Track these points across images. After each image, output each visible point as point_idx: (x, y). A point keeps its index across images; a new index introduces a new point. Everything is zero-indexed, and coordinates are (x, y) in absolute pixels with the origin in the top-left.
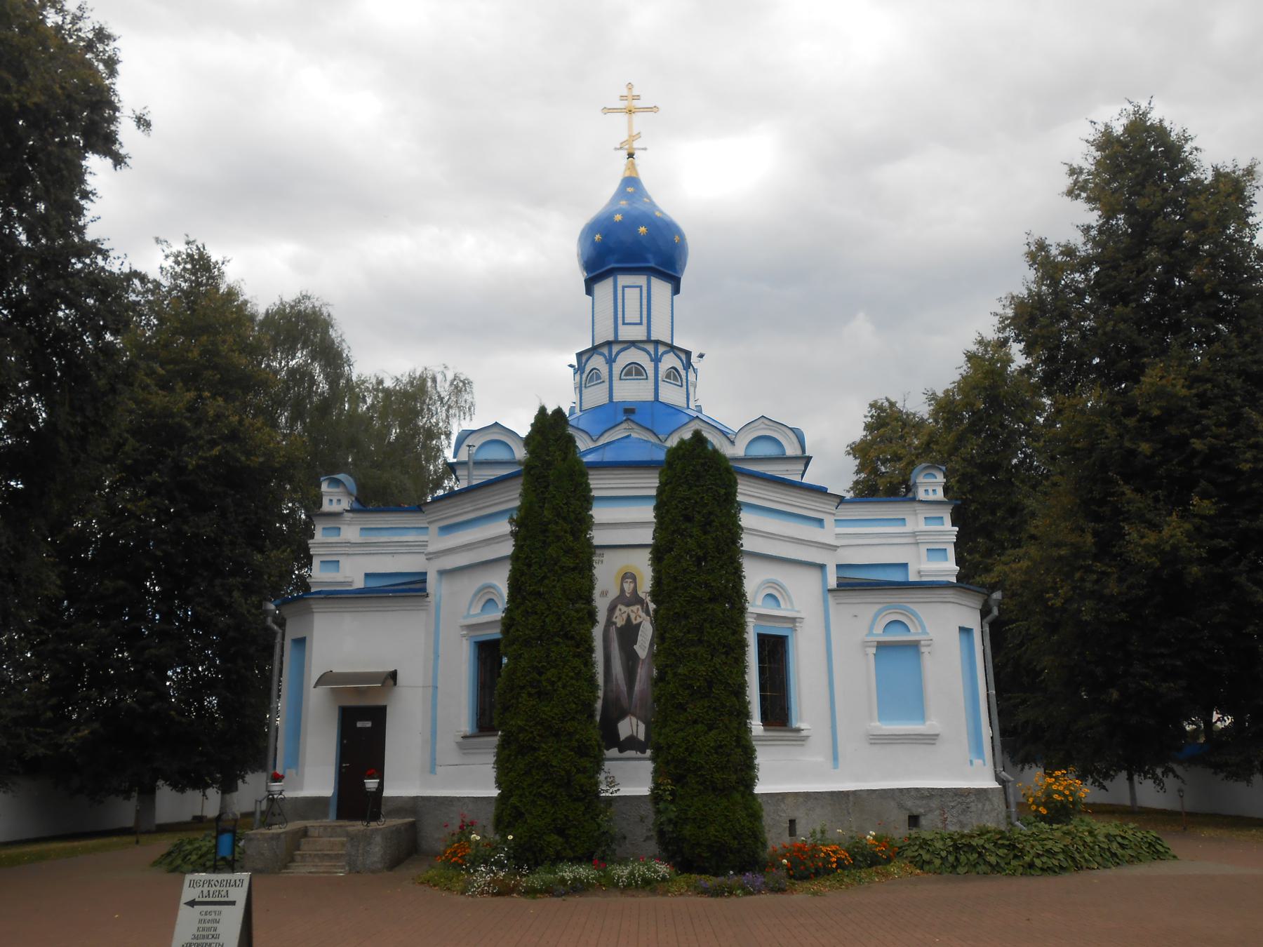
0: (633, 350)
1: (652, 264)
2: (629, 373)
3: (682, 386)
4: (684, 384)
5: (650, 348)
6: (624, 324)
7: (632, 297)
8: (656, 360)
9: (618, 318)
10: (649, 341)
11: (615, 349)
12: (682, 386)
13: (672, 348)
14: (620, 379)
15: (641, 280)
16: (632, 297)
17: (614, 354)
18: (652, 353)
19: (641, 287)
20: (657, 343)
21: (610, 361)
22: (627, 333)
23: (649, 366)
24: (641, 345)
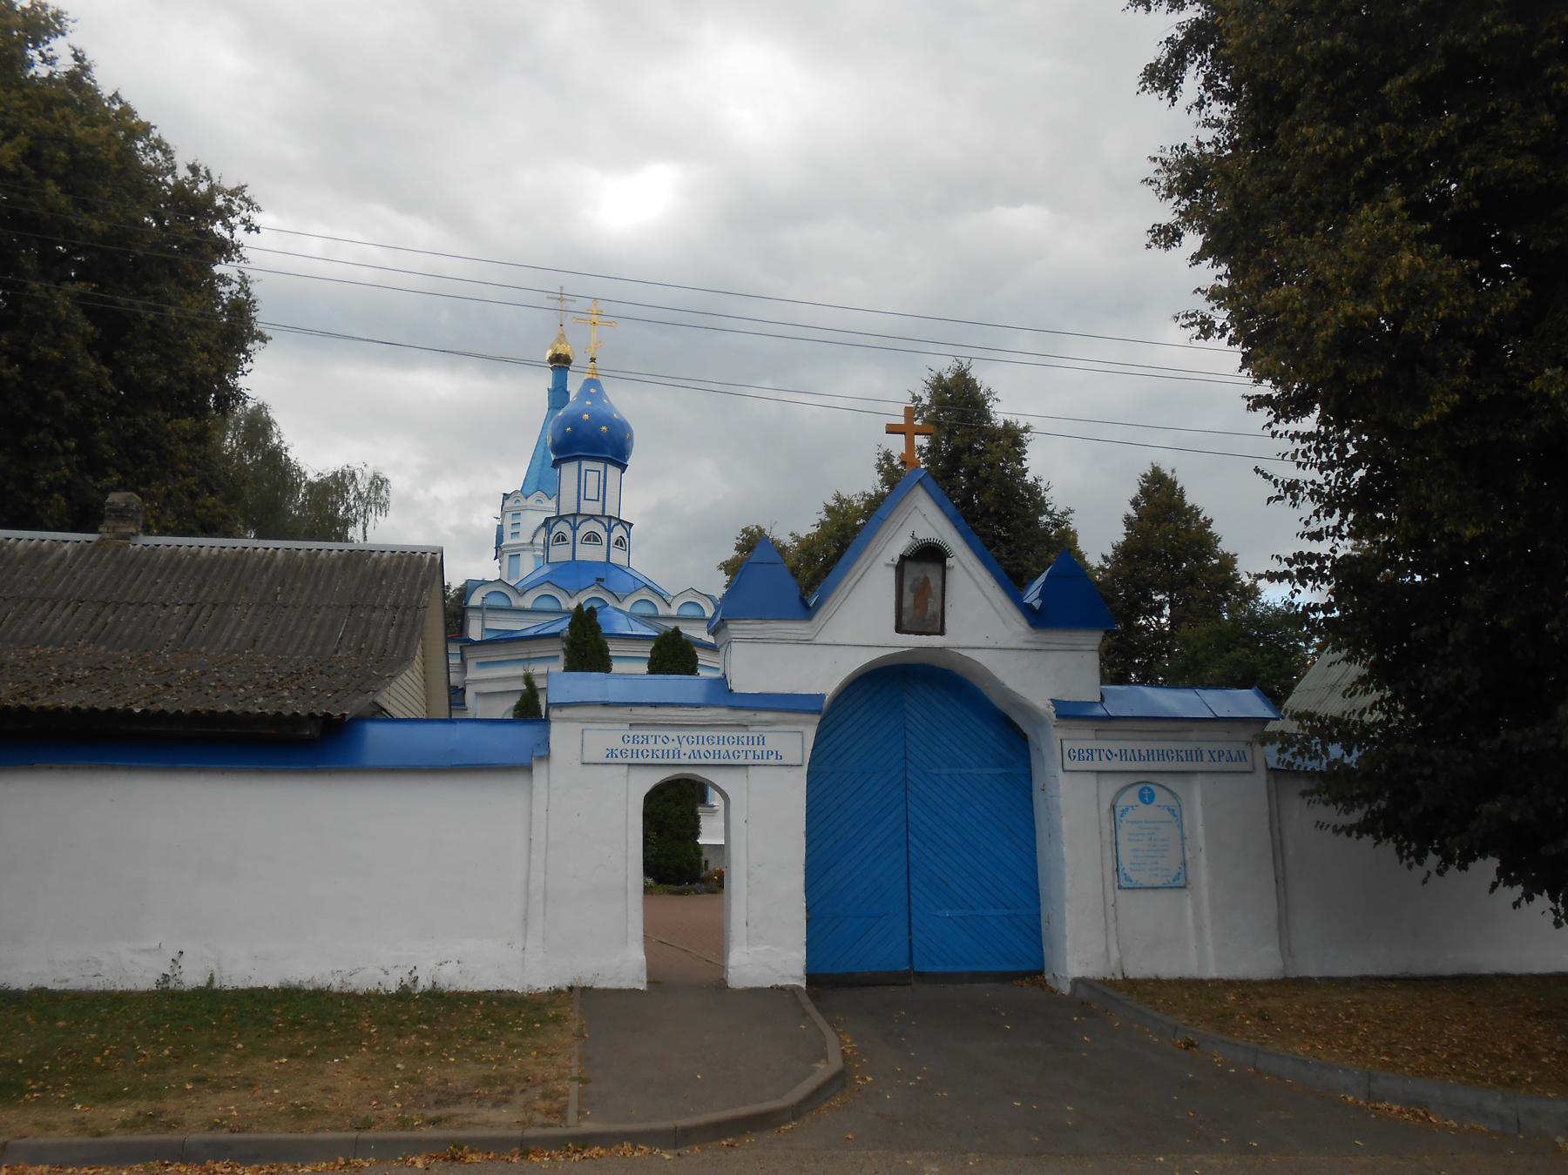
3: (625, 550)
5: (571, 520)
6: (585, 499)
8: (574, 529)
10: (603, 516)
13: (621, 522)
16: (592, 478)
20: (610, 518)
22: (589, 508)
23: (569, 534)
24: (567, 519)
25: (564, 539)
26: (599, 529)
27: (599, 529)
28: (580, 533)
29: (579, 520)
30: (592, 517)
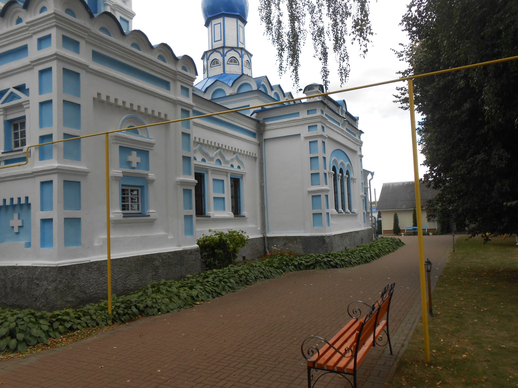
1: (224, 12)
2: (214, 64)
4: (240, 64)
7: (218, 28)
8: (224, 56)
9: (213, 40)
11: (208, 54)
12: (239, 65)
14: (211, 67)
15: (220, 20)
17: (208, 56)
18: (222, 53)
21: (208, 59)
24: (218, 50)
25: (217, 63)
26: (237, 56)
27: (237, 56)
28: (227, 58)
29: (226, 50)
30: (232, 48)
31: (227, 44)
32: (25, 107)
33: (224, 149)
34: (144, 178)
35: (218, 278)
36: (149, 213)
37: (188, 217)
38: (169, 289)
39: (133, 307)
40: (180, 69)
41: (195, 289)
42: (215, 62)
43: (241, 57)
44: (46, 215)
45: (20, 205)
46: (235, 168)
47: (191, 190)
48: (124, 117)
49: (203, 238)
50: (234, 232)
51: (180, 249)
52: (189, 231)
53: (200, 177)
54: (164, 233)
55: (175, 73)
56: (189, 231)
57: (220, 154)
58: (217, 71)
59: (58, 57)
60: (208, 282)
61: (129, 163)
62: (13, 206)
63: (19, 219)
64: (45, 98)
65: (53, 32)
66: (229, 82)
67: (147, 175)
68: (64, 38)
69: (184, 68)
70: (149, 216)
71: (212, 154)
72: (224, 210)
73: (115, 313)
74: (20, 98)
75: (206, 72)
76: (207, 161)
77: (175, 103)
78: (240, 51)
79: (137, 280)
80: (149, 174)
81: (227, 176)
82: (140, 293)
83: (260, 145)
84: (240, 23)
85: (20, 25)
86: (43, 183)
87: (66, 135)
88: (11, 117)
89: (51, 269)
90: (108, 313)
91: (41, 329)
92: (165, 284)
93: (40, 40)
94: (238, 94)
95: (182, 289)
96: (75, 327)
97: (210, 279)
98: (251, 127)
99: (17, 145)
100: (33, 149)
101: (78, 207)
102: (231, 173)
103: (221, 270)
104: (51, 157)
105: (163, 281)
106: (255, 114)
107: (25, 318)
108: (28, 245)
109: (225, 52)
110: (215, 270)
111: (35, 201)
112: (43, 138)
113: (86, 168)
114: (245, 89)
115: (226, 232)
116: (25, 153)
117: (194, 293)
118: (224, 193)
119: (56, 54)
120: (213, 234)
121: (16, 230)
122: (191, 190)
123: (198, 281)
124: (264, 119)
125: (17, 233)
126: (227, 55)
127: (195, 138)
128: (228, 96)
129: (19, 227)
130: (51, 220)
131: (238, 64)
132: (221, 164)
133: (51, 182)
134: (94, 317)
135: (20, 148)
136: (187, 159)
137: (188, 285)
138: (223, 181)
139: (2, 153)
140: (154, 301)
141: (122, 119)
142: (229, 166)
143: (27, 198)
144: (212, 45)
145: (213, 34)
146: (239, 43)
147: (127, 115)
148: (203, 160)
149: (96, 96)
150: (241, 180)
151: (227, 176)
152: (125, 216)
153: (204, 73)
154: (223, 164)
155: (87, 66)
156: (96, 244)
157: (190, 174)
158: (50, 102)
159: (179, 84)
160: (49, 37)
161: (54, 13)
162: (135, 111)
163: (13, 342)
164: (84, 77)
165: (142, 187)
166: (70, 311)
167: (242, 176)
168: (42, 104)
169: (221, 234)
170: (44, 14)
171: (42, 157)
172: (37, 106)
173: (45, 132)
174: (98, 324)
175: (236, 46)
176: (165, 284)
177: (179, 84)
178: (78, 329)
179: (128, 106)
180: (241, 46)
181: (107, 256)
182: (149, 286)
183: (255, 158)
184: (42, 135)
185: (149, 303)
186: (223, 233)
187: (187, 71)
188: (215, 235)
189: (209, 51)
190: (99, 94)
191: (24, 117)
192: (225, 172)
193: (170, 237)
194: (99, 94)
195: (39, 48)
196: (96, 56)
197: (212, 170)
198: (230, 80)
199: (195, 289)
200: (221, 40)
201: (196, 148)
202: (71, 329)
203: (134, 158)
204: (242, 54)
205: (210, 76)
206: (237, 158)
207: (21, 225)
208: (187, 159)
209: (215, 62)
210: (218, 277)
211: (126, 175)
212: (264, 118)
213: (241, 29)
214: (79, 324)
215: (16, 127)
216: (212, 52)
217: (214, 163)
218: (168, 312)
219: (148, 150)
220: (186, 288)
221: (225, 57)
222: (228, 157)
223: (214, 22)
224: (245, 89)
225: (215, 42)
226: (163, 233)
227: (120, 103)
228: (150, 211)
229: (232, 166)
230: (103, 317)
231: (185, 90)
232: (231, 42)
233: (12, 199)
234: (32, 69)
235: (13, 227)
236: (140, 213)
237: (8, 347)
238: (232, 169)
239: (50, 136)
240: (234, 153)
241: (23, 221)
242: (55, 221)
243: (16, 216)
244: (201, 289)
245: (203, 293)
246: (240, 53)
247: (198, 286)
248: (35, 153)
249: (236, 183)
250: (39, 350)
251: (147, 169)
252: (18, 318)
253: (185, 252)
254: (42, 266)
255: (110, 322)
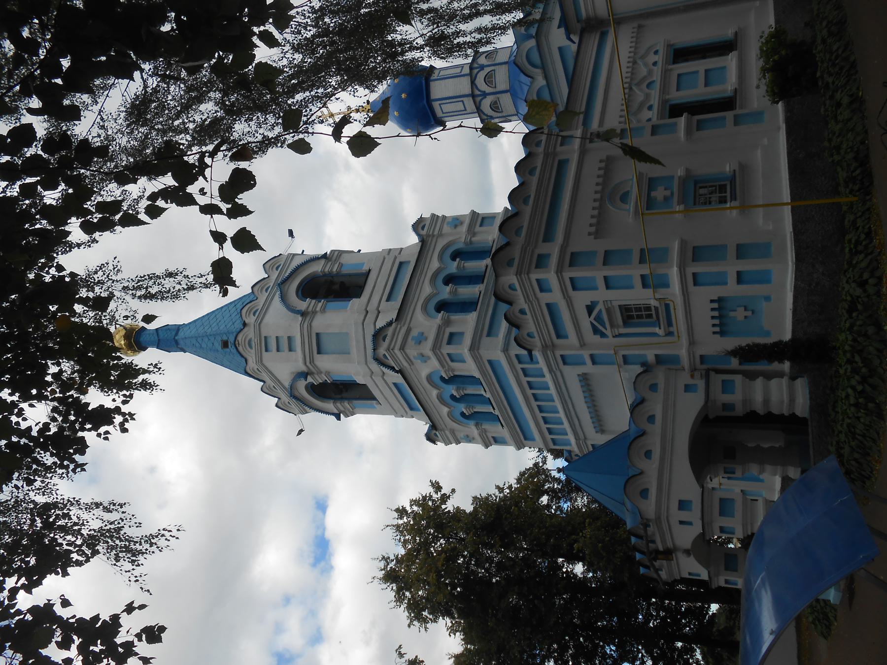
0: (482, 108)
4: (492, 68)
5: (478, 99)
7: (447, 108)
8: (485, 95)
9: (463, 113)
12: (494, 70)
14: (502, 112)
15: (436, 105)
18: (480, 98)
19: (440, 104)
25: (495, 103)
28: (488, 90)
29: (477, 92)
31: (467, 90)
32: (610, 306)
33: (631, 80)
34: (683, 181)
35: (830, 69)
36: (730, 172)
37: (737, 121)
38: (837, 134)
39: (854, 175)
40: (541, 149)
41: (841, 99)
42: (495, 106)
43: (482, 67)
44: (732, 279)
45: (719, 309)
46: (658, 58)
47: (698, 121)
48: (611, 207)
49: (769, 96)
50: (761, 49)
51: (783, 127)
52: (757, 116)
53: (676, 111)
54: (759, 151)
55: (547, 155)
56: (757, 116)
57: (638, 84)
58: (506, 101)
59: (559, 271)
60: (833, 83)
61: (666, 199)
62: (720, 317)
63: (735, 311)
64: (601, 284)
65: (534, 277)
66: (522, 82)
67: (679, 178)
68: (537, 267)
69: (538, 144)
70: (734, 170)
71: (639, 96)
72: (725, 67)
73: (857, 193)
74: (600, 311)
75: (509, 118)
76: (652, 103)
77: (583, 152)
78: (475, 71)
79: (823, 178)
80: (679, 174)
81: (671, 70)
82: (839, 169)
83: (619, 22)
84: (435, 76)
85: (527, 311)
86: (695, 284)
87: (642, 261)
88: (620, 321)
89: (798, 270)
90: (857, 201)
91: (863, 260)
92: (830, 141)
93: (542, 290)
94: (544, 68)
95: (839, 118)
96: (866, 230)
97: (830, 80)
98: (593, 41)
99: (650, 316)
100: (658, 296)
101: (724, 247)
102: (666, 63)
103: (820, 64)
104: (666, 275)
105: (826, 144)
106: (572, 37)
107: (848, 276)
108: (768, 299)
109: (480, 93)
110: (818, 74)
111: (716, 292)
112: (645, 285)
113: (677, 242)
114: (536, 58)
115: (761, 63)
116: (660, 303)
117: (846, 100)
118: (697, 72)
119: (557, 273)
120: (764, 81)
121: (749, 313)
122: (698, 121)
123: (832, 97)
124: (578, 21)
125: (753, 312)
126: (483, 90)
127: (620, 123)
128: (547, 82)
129: (746, 309)
130: (739, 273)
131: (493, 72)
132: (654, 81)
133: (694, 274)
134: (860, 214)
135: (653, 312)
136: (655, 130)
137: (834, 109)
138: (679, 75)
139: (660, 328)
140: (849, 150)
141: (613, 209)
142: (655, 68)
143: (712, 301)
144: (470, 113)
145: (456, 113)
146: (462, 73)
147: (608, 205)
148: (650, 108)
149: (593, 237)
150: (677, 47)
151: (671, 70)
152: (734, 198)
153: (511, 121)
154: (655, 79)
155: (562, 246)
156: (771, 227)
157: (675, 124)
158: (606, 278)
159: (559, 149)
160: (538, 280)
161: (516, 275)
162: (602, 197)
163: (872, 281)
164: (574, 247)
165: (696, 183)
166: (847, 237)
167: (669, 46)
168: (608, 287)
169: (764, 70)
170: (517, 286)
171: (666, 285)
172: (609, 291)
173: (638, 282)
174: (868, 209)
175: (469, 78)
176: (830, 141)
177: (559, 149)
178: (870, 228)
179: (597, 204)
180: (466, 70)
181: (786, 207)
182: (830, 160)
183: (640, 27)
184: (641, 286)
185: (851, 156)
186: (763, 67)
187: (541, 141)
188: (765, 79)
189: (480, 116)
190: (590, 234)
191: (620, 306)
192: (666, 73)
193: (765, 141)
194: (590, 234)
195: (550, 291)
196: (548, 237)
197: (663, 94)
198: (520, 82)
199: (841, 99)
200: (462, 101)
201: (633, 120)
202: (868, 234)
203: (659, 193)
204: (477, 68)
205: (514, 111)
206: (642, 57)
207: (743, 308)
208: (655, 130)
209: (495, 106)
210: (828, 69)
211: (682, 200)
212: (576, 21)
213: (442, 73)
214: (863, 227)
215: (630, 317)
216: (481, 113)
217: (653, 92)
218: (866, 132)
219: (648, 180)
220: (839, 112)
221: (487, 92)
222: (643, 71)
223: (439, 114)
224: (536, 58)
225: (465, 110)
226: (759, 153)
227: (596, 212)
228: (728, 169)
229: (655, 64)
230: (860, 205)
231: (565, 140)
232: (464, 85)
233: (713, 317)
234: (569, 297)
235: (746, 317)
236: (731, 182)
237: (875, 285)
238: (660, 64)
239: (643, 277)
240: (635, 63)
241: (738, 306)
242: (740, 268)
243: (732, 314)
244: (842, 91)
245: (848, 88)
246: (478, 70)
247: (838, 96)
248: (662, 293)
249: (681, 54)
250: (884, 257)
251: (673, 177)
252: (847, 282)
253: (788, 121)
254: (793, 280)
255: (868, 198)
